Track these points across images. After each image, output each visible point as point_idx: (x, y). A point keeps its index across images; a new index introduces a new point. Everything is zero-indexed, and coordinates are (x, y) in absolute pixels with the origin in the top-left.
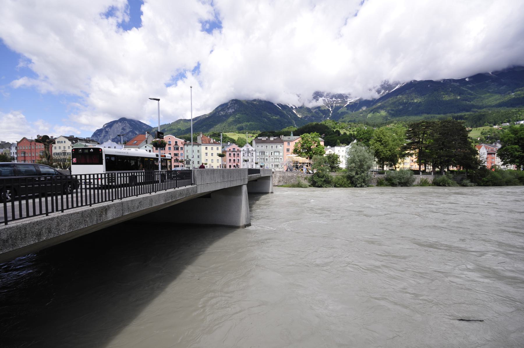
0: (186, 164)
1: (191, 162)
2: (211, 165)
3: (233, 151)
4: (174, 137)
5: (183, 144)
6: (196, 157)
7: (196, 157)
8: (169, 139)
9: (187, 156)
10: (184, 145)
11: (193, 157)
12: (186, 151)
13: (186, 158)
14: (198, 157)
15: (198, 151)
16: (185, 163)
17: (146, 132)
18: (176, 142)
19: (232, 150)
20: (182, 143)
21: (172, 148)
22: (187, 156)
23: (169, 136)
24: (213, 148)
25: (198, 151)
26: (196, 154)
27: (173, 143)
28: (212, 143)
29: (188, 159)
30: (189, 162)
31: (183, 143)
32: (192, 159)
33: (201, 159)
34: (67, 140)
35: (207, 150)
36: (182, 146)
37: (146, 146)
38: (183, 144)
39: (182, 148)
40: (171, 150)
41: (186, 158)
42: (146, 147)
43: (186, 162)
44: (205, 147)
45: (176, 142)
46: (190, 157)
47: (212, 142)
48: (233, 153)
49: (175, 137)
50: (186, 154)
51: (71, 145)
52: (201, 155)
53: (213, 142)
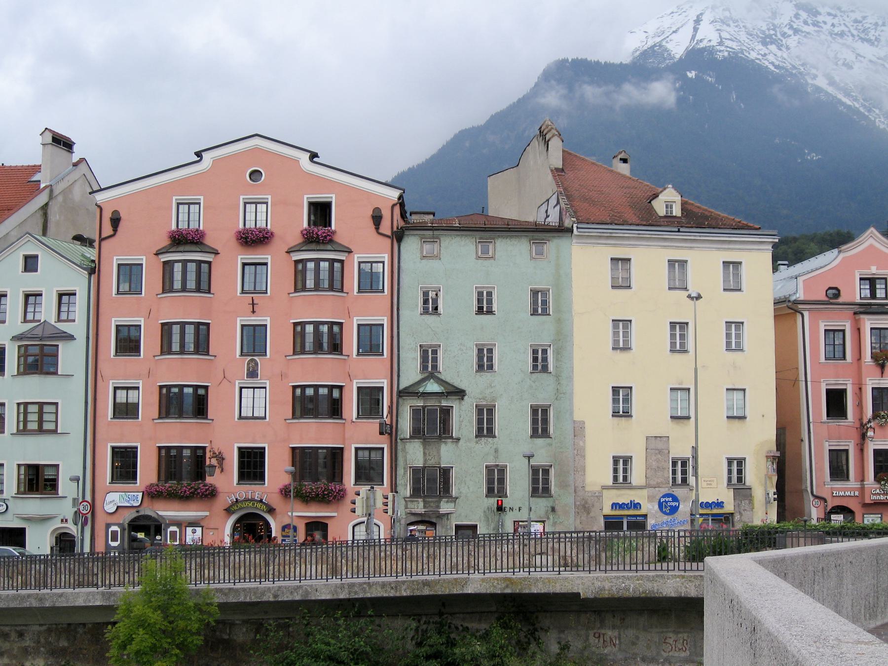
0: (417, 433)
2: (663, 452)
3: (866, 309)
5: (386, 228)
10: (398, 236)
13: (411, 374)
16: (406, 425)
19: (856, 293)
20: (377, 219)
23: (257, 150)
24: (683, 263)
28: (669, 219)
29: (432, 387)
30: (446, 412)
31: (386, 214)
38: (386, 228)
41: (411, 374)
42: (30, 264)
43: (416, 412)
47: (669, 206)
48: (868, 323)
52: (563, 339)
53: (677, 211)
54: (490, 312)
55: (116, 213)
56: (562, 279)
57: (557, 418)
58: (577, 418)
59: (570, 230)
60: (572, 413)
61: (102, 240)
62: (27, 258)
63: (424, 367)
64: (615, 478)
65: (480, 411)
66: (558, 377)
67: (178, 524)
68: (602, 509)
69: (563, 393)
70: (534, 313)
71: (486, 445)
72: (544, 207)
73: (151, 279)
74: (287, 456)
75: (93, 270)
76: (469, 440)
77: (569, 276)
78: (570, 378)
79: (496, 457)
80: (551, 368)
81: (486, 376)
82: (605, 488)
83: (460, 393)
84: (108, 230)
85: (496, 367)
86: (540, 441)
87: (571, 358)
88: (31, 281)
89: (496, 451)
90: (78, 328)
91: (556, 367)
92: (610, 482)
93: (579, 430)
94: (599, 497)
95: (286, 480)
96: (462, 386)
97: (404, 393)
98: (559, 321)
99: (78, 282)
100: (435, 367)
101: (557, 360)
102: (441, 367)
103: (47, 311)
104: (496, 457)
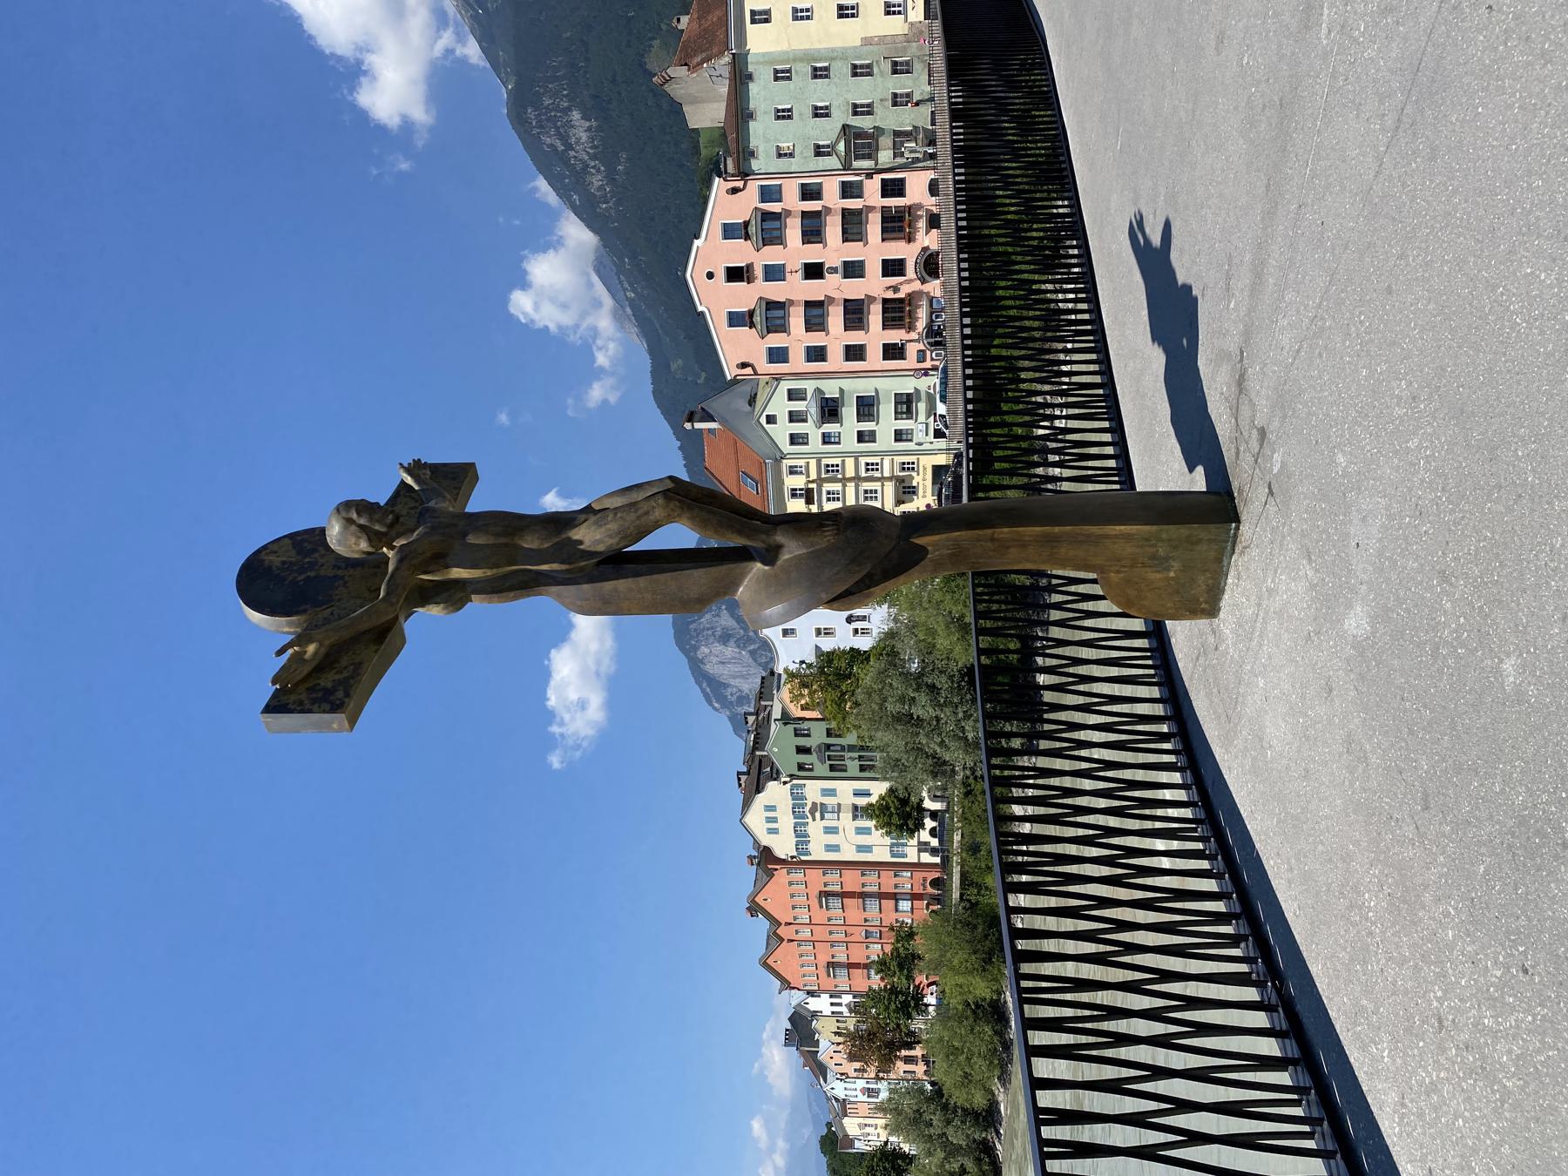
0: (869, 157)
1: (864, 123)
4: (697, 243)
5: (740, 184)
6: (820, 93)
7: (820, 93)
8: (710, 276)
9: (819, 151)
11: (820, 113)
12: (783, 165)
13: (833, 162)
14: (819, 73)
15: (781, 75)
16: (867, 164)
17: (688, 426)
18: (729, 231)
20: (735, 191)
21: (772, 255)
22: (819, 151)
25: (781, 75)
26: (805, 92)
27: (741, 252)
29: (841, 147)
31: (731, 185)
32: (841, 117)
33: (835, 55)
34: (761, 800)
35: (768, 12)
36: (753, 187)
37: (763, 420)
38: (740, 184)
39: (768, 194)
40: (784, 265)
42: (771, 419)
44: (752, 30)
45: (729, 231)
46: (826, 132)
49: (697, 236)
50: (804, 161)
51: (785, 783)
52: (806, 56)
54: (790, 110)
55: (738, 366)
56: (768, 59)
57: (859, 58)
58: (858, 43)
59: (733, 54)
60: (856, 47)
61: (756, 373)
62: (768, 422)
63: (829, 154)
64: (899, 13)
65: (855, 113)
66: (832, 59)
67: (932, 313)
68: (920, 22)
69: (841, 54)
70: (789, 78)
71: (878, 109)
72: (714, 79)
73: (776, 340)
74: (887, 244)
75: (778, 378)
76: (875, 119)
77: (764, 55)
78: (833, 50)
79: (886, 100)
80: (826, 64)
81: (834, 112)
82: (906, 20)
83: (845, 127)
84: (749, 370)
85: (827, 104)
86: (875, 70)
87: (818, 50)
88: (783, 418)
89: (881, 100)
90: (809, 386)
91: (825, 61)
92: (902, 17)
93: (867, 41)
94: (912, 24)
95: (902, 244)
96: (840, 126)
97: (847, 167)
98: (795, 60)
99: (785, 386)
100: (828, 146)
101: (820, 60)
102: (828, 142)
103: (799, 406)
104: (886, 100)
